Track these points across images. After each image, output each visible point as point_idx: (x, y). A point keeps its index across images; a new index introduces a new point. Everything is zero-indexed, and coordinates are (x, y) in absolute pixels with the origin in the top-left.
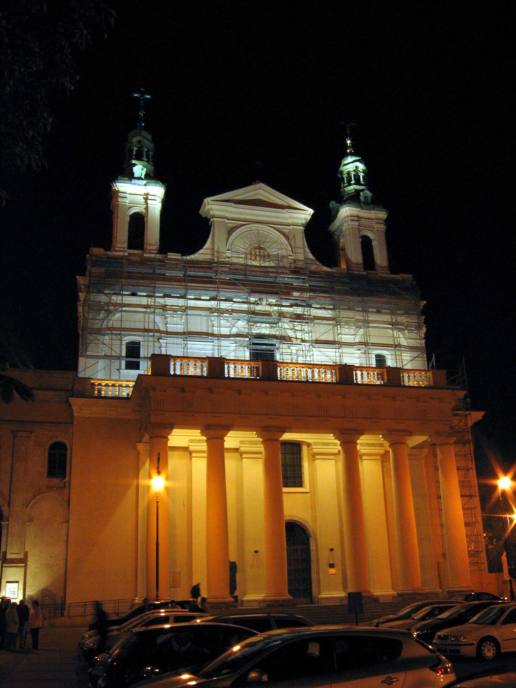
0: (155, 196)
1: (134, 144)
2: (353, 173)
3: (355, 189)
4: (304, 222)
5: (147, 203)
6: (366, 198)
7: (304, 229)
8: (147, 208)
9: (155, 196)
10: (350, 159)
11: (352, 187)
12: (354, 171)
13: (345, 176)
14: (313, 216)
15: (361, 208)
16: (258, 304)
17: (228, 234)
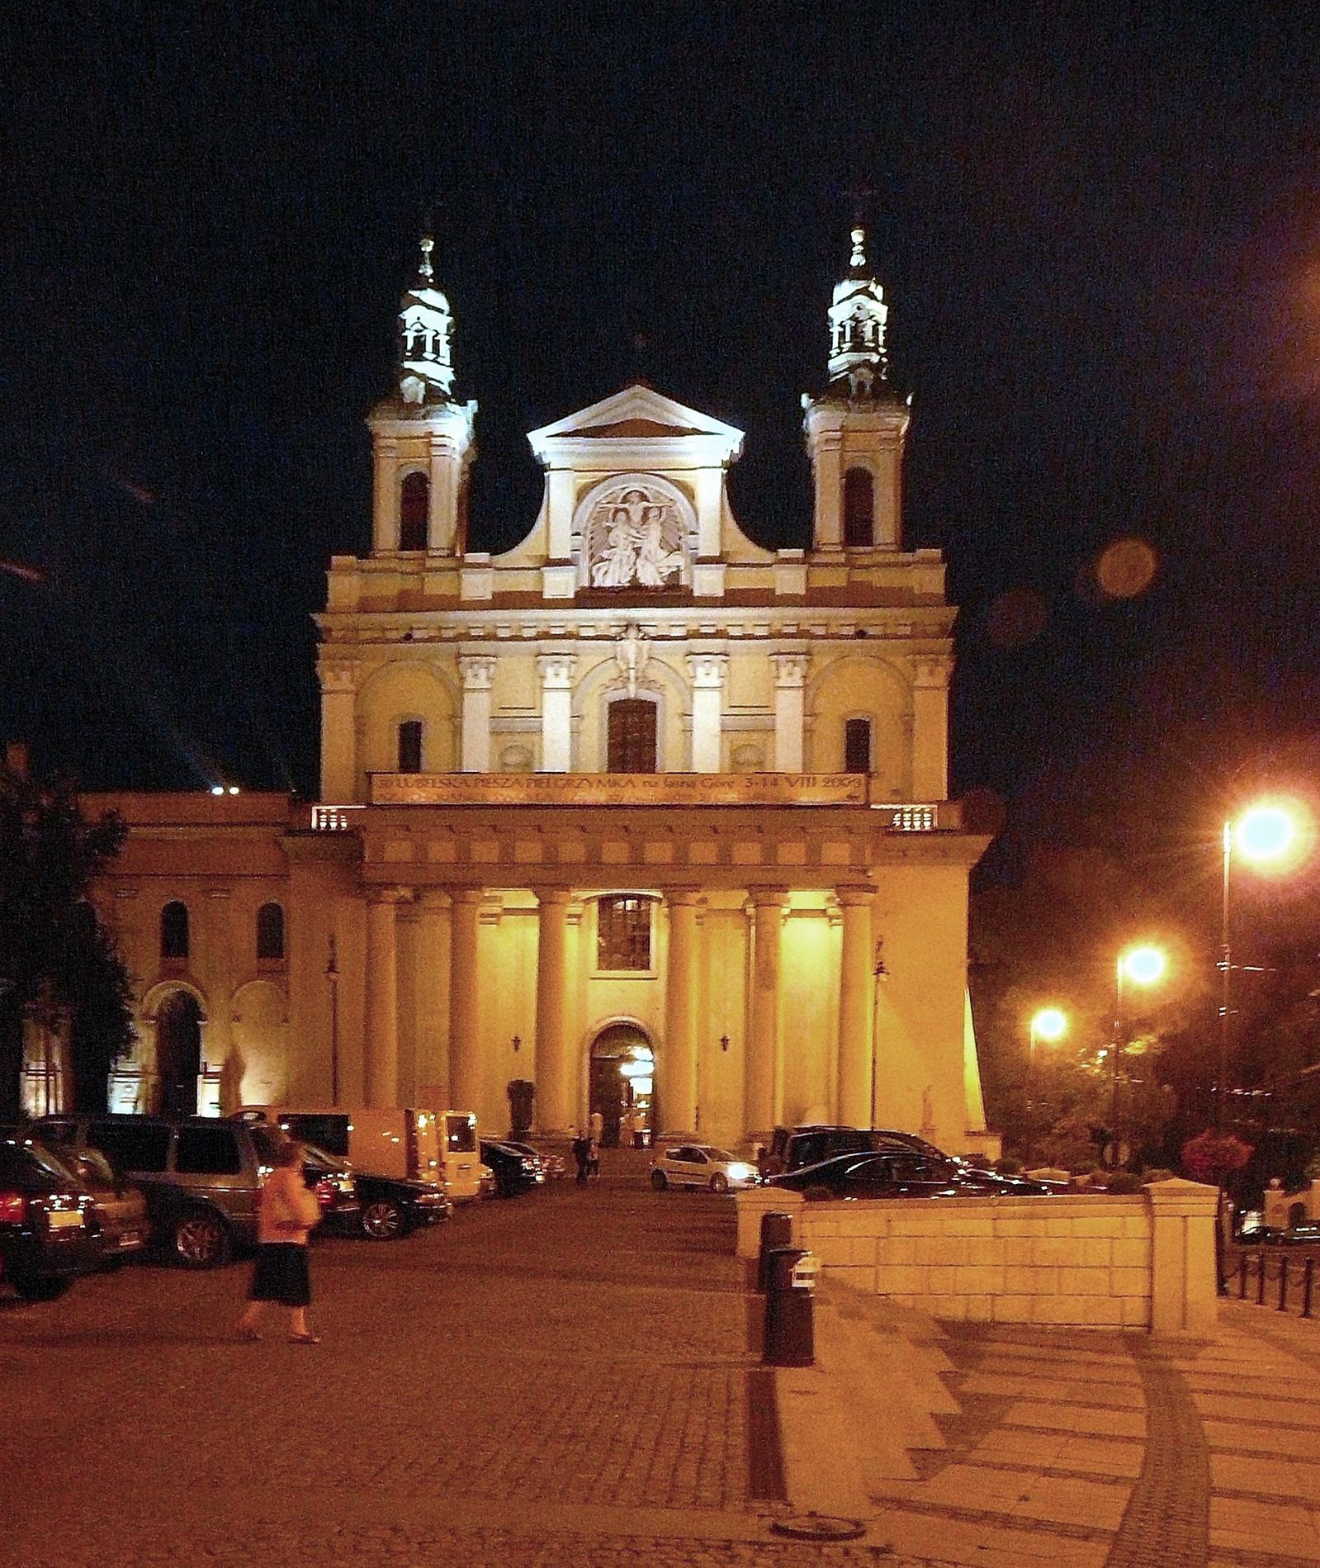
0: (443, 436)
1: (408, 326)
2: (849, 324)
3: (848, 361)
4: (726, 458)
5: (429, 456)
6: (861, 385)
7: (726, 471)
8: (429, 466)
9: (443, 436)
10: (843, 289)
11: (843, 358)
12: (852, 318)
13: (835, 330)
14: (747, 443)
15: (849, 410)
16: (621, 639)
17: (578, 499)
